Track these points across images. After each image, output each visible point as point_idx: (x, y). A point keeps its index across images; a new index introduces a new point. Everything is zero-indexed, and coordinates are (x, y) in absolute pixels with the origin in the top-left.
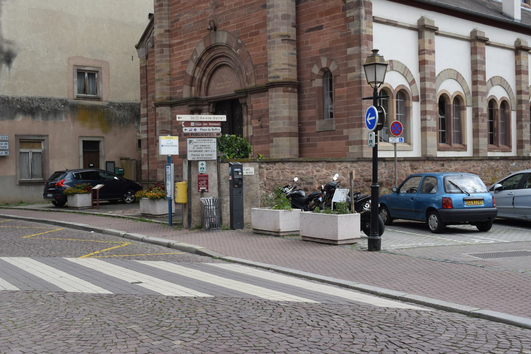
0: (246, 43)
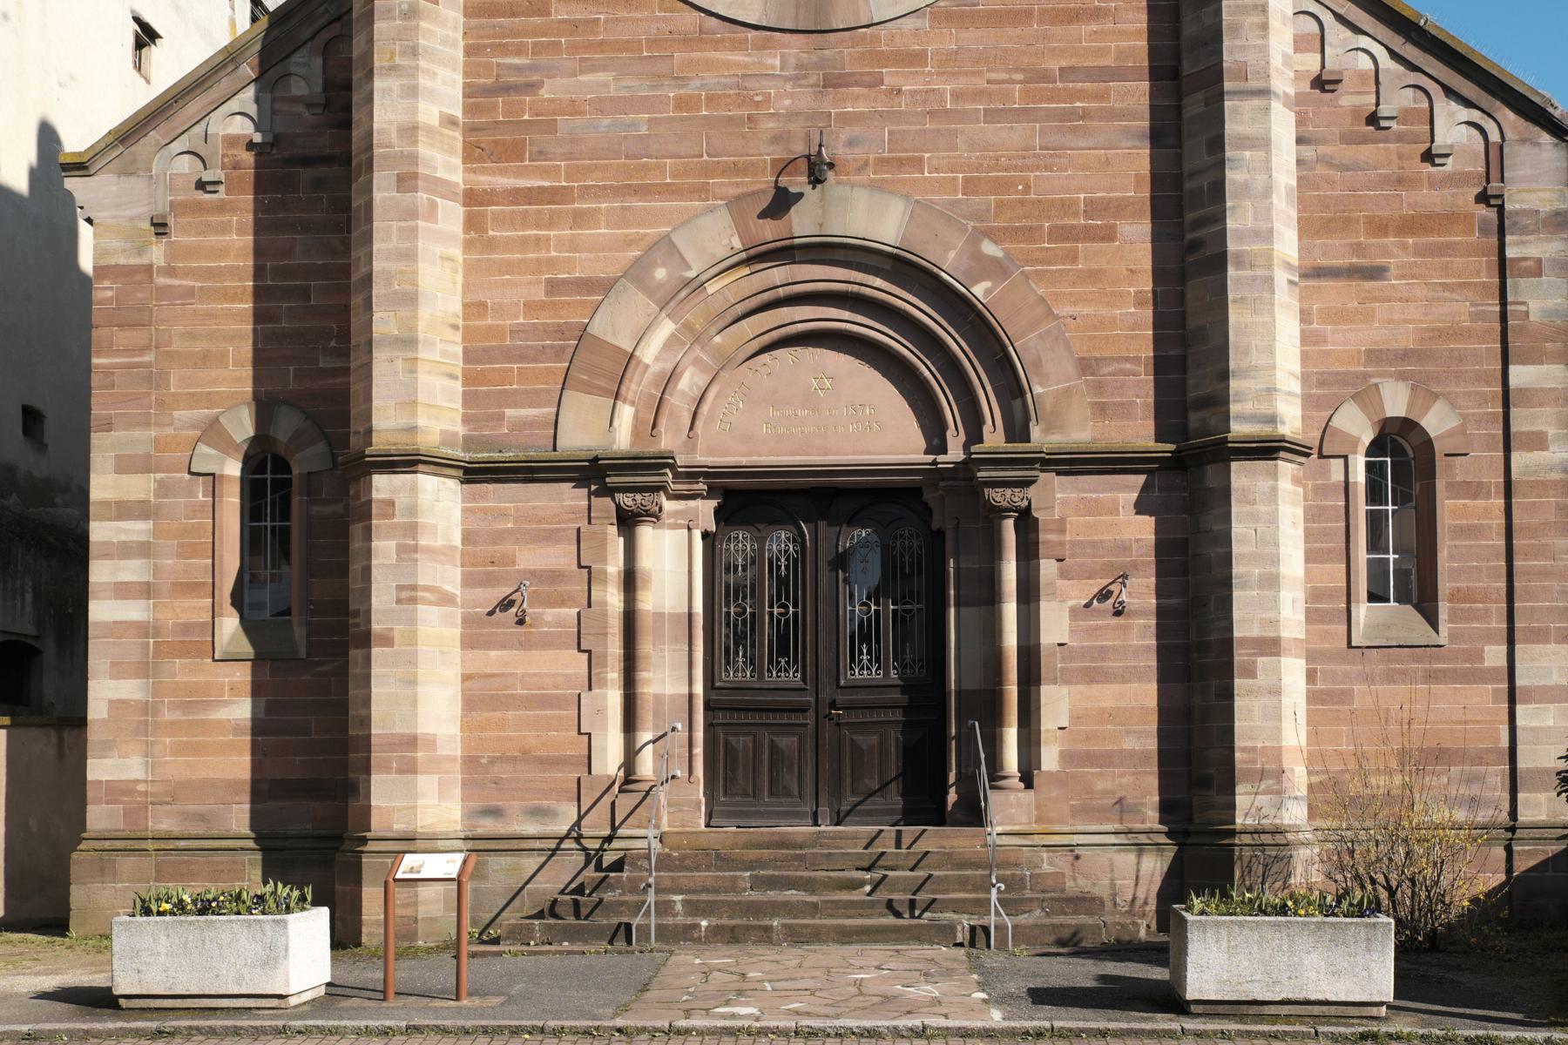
0: (1027, 262)
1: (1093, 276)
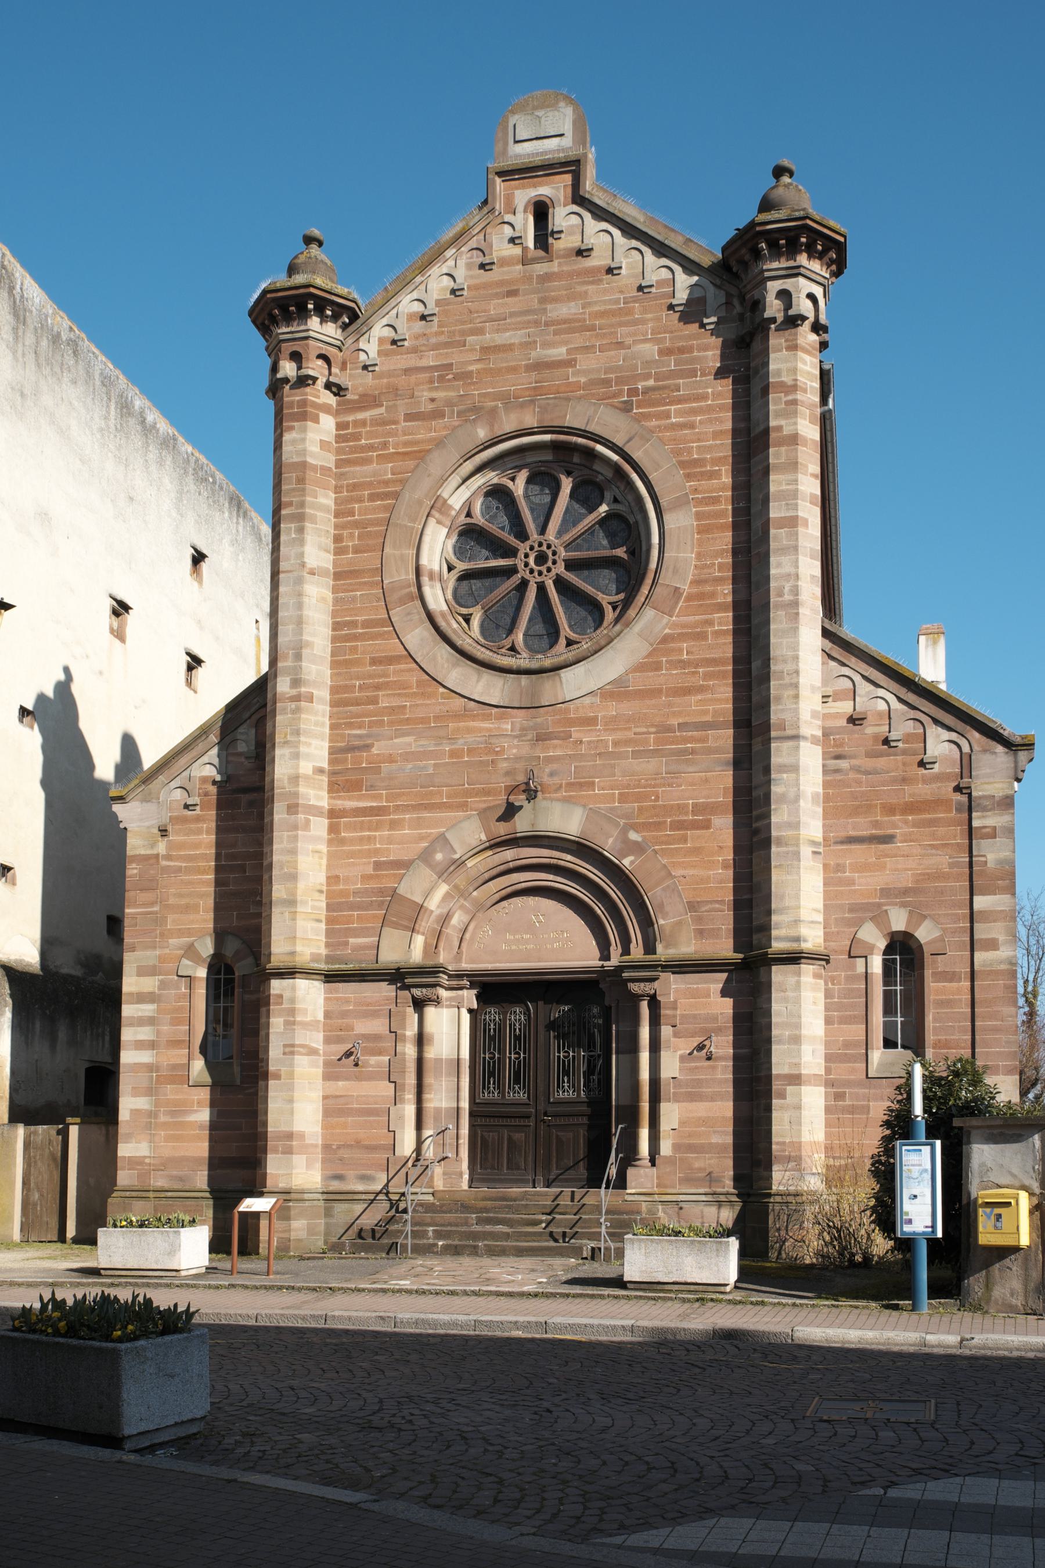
0: (656, 844)
1: (696, 851)
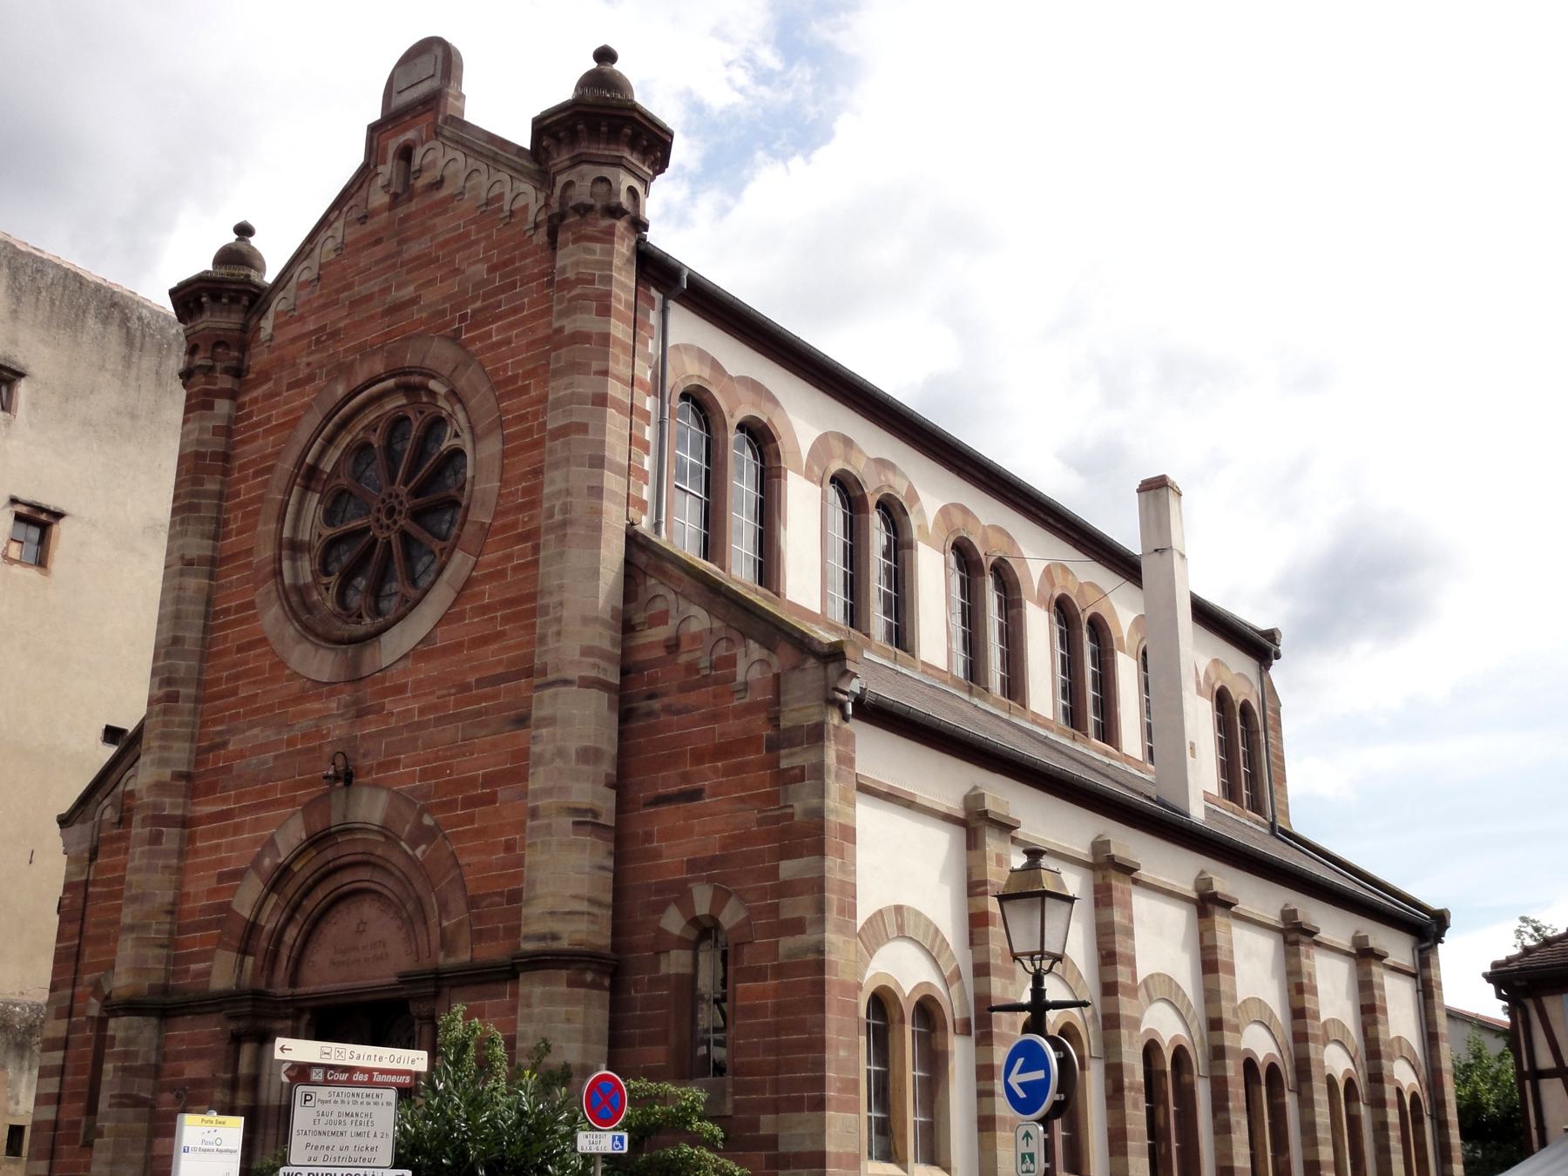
1: (480, 833)
